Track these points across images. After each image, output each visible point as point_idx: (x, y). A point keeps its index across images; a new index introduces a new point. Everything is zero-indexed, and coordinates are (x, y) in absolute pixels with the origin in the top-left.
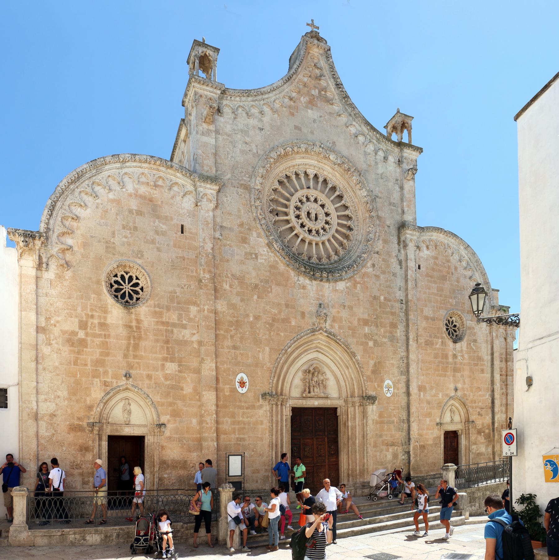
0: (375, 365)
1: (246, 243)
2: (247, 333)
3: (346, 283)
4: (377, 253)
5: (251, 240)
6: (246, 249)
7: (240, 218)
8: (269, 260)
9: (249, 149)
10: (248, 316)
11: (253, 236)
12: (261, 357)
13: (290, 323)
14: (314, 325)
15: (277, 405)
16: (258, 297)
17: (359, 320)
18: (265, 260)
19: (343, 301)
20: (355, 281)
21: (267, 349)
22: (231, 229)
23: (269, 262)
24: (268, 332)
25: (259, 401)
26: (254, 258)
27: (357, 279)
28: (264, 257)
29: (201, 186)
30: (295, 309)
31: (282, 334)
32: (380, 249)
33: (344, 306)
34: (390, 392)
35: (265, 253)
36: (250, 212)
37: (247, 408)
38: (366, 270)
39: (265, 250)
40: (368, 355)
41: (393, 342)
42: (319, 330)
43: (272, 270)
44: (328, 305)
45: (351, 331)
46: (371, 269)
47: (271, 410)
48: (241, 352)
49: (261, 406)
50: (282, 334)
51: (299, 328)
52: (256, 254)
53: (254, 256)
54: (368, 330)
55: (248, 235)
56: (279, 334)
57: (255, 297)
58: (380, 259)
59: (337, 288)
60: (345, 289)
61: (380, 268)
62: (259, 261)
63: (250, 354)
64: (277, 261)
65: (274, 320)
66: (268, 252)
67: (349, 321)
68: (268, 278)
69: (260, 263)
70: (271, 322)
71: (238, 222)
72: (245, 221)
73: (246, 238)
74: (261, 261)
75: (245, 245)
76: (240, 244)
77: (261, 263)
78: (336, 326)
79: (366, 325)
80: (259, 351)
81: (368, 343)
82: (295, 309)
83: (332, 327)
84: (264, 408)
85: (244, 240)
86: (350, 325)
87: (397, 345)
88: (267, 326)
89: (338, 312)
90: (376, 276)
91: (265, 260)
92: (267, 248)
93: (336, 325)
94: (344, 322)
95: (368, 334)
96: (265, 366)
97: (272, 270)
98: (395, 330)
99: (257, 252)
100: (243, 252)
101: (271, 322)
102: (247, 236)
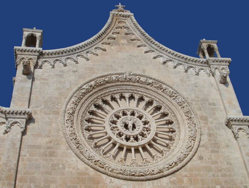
1: (54, 156)
3: (170, 178)
4: (203, 146)
6: (54, 161)
7: (49, 137)
22: (39, 147)
27: (182, 173)
29: (10, 118)
35: (73, 162)
36: (60, 131)
39: (74, 159)
46: (199, 162)
53: (61, 166)
59: (159, 185)
62: (67, 169)
64: (86, 168)
66: (77, 161)
68: (75, 184)
71: (47, 140)
72: (55, 138)
73: (54, 152)
75: (52, 158)
76: (48, 158)
85: (52, 154)
91: (74, 168)
92: (76, 157)
97: (80, 176)
100: (50, 165)
102: (56, 150)
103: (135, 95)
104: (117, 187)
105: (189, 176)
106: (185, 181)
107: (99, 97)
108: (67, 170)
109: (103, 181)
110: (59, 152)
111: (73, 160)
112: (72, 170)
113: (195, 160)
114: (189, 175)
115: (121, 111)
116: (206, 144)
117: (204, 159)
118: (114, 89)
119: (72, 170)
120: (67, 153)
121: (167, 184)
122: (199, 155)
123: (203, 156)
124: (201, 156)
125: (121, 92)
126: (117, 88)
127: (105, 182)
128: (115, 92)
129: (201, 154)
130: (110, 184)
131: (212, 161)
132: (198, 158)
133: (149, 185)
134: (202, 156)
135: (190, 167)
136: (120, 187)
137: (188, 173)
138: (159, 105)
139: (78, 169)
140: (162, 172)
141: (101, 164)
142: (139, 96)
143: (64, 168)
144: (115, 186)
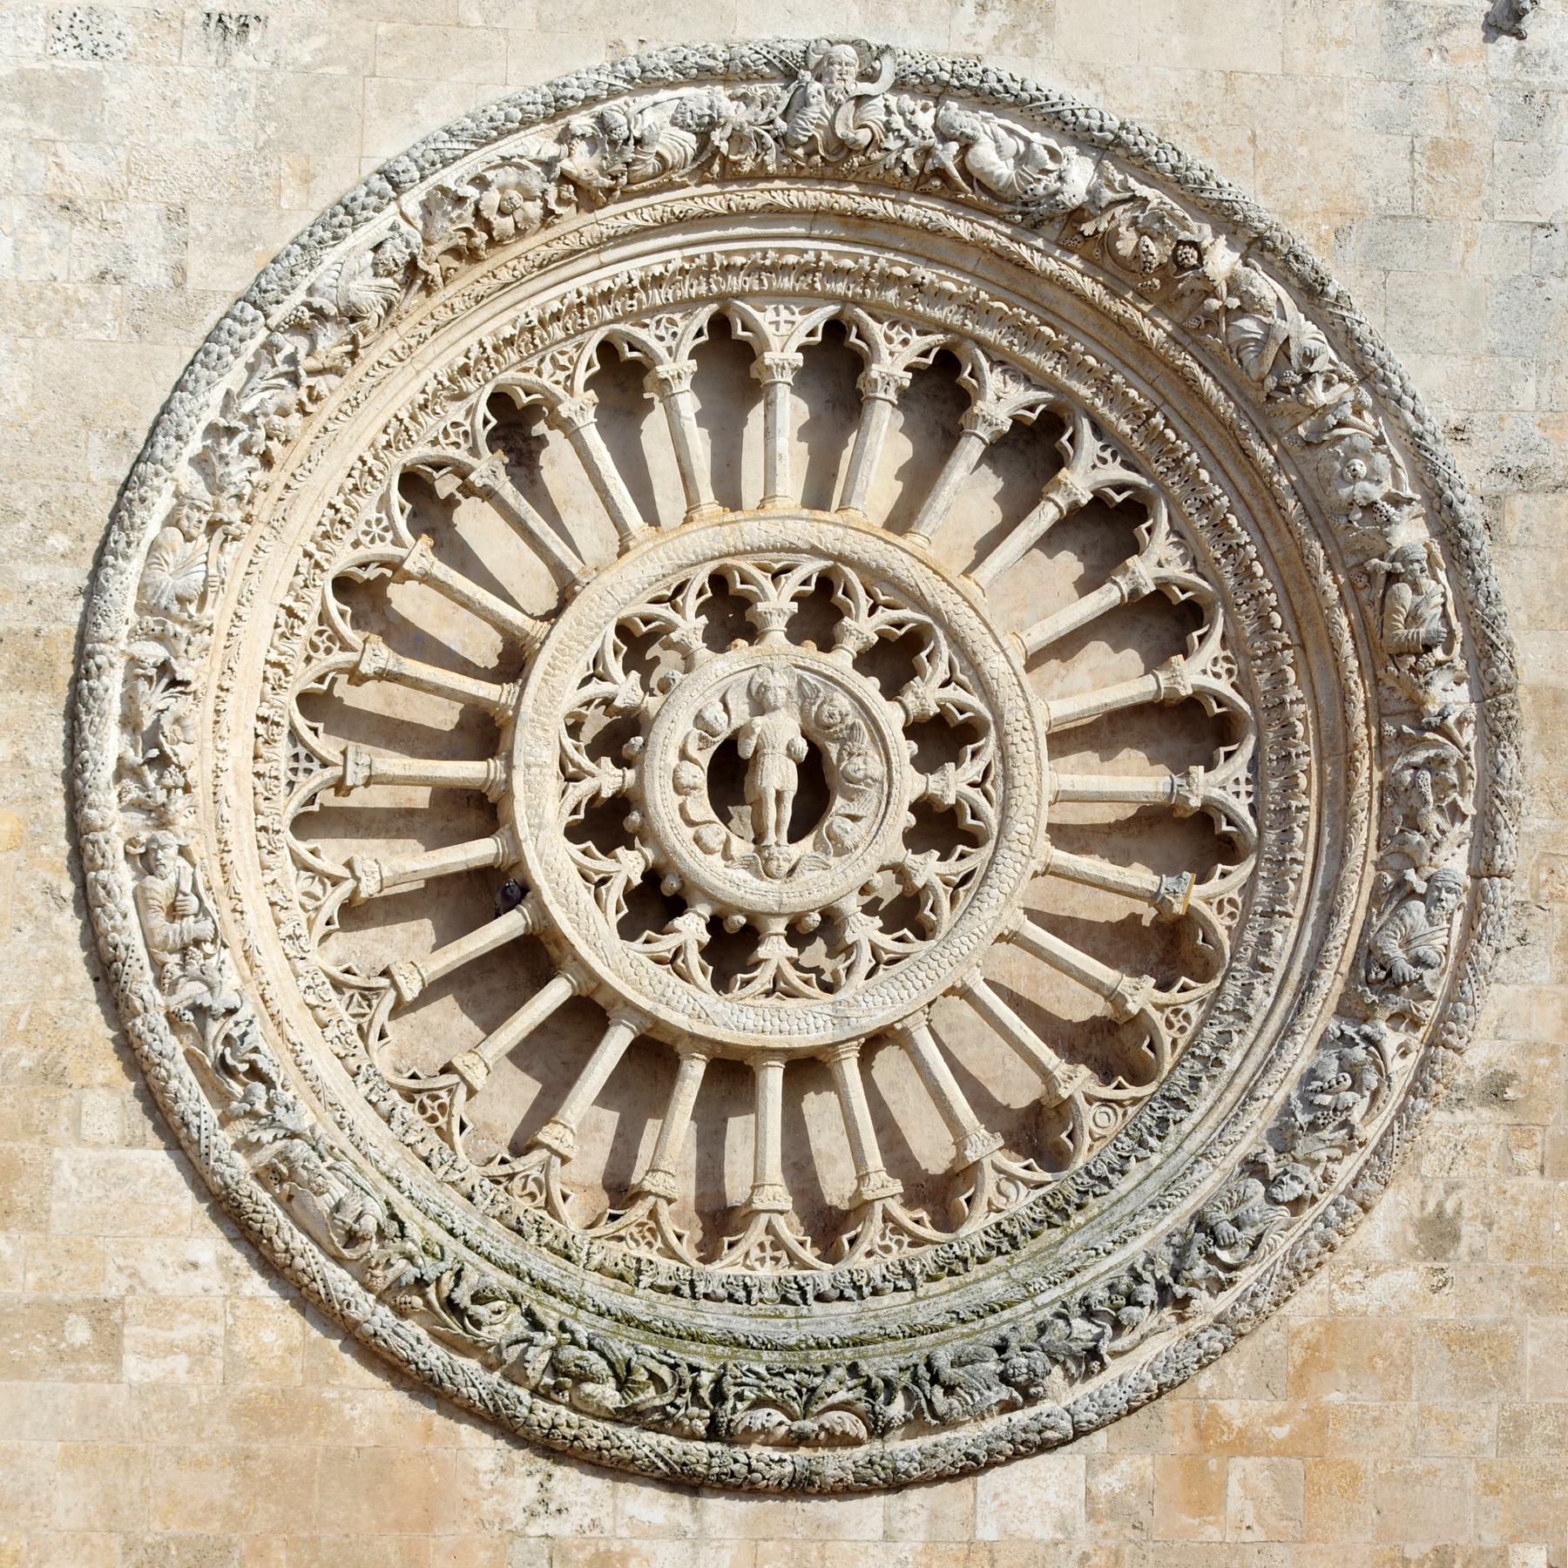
3: (1091, 1467)
5: (65, 1177)
8: (243, 1345)
9: (91, 265)
11: (88, 1132)
18: (200, 1354)
20: (1207, 1428)
23: (235, 1366)
26: (77, 1352)
27: (1231, 1409)
28: (187, 1330)
32: (1529, 1048)
35: (196, 1281)
38: (1343, 1300)
43: (262, 1447)
46: (1410, 1278)
52: (102, 1314)
55: (28, 1129)
58: (1525, 1157)
60: (1083, 1529)
61: (1512, 1250)
62: (134, 1368)
69: (141, 1393)
74: (157, 1370)
77: (155, 1388)
90: (1461, 1340)
91: (200, 1354)
97: (262, 1447)
99: (114, 1287)
102: (29, 1148)
103: (878, 330)
104: (597, 1554)
105: (1281, 1450)
106: (1234, 1488)
107: (467, 384)
108: (135, 1377)
109: (470, 1493)
110: (59, 1161)
111: (195, 1266)
112: (182, 1376)
113: (1384, 1254)
114: (1280, 1432)
115: (701, 577)
116: (1523, 1073)
117: (1463, 1249)
118: (634, 270)
119: (182, 1376)
120: (140, 1174)
121: (1062, 1526)
122: (1423, 1203)
123: (1466, 1213)
124: (1449, 1207)
125: (723, 298)
126: (680, 247)
127: (487, 1505)
128: (658, 296)
129: (1451, 1189)
130: (535, 1529)
131: (1533, 1272)
132: (1411, 1237)
133: (888, 1537)
134: (1458, 1212)
135: (1307, 1335)
136: (624, 1558)
137: (1279, 1407)
138: (1120, 488)
139: (235, 1366)
140: (1031, 1400)
141: (451, 1305)
142: (918, 342)
143: (109, 1346)
144: (581, 1548)
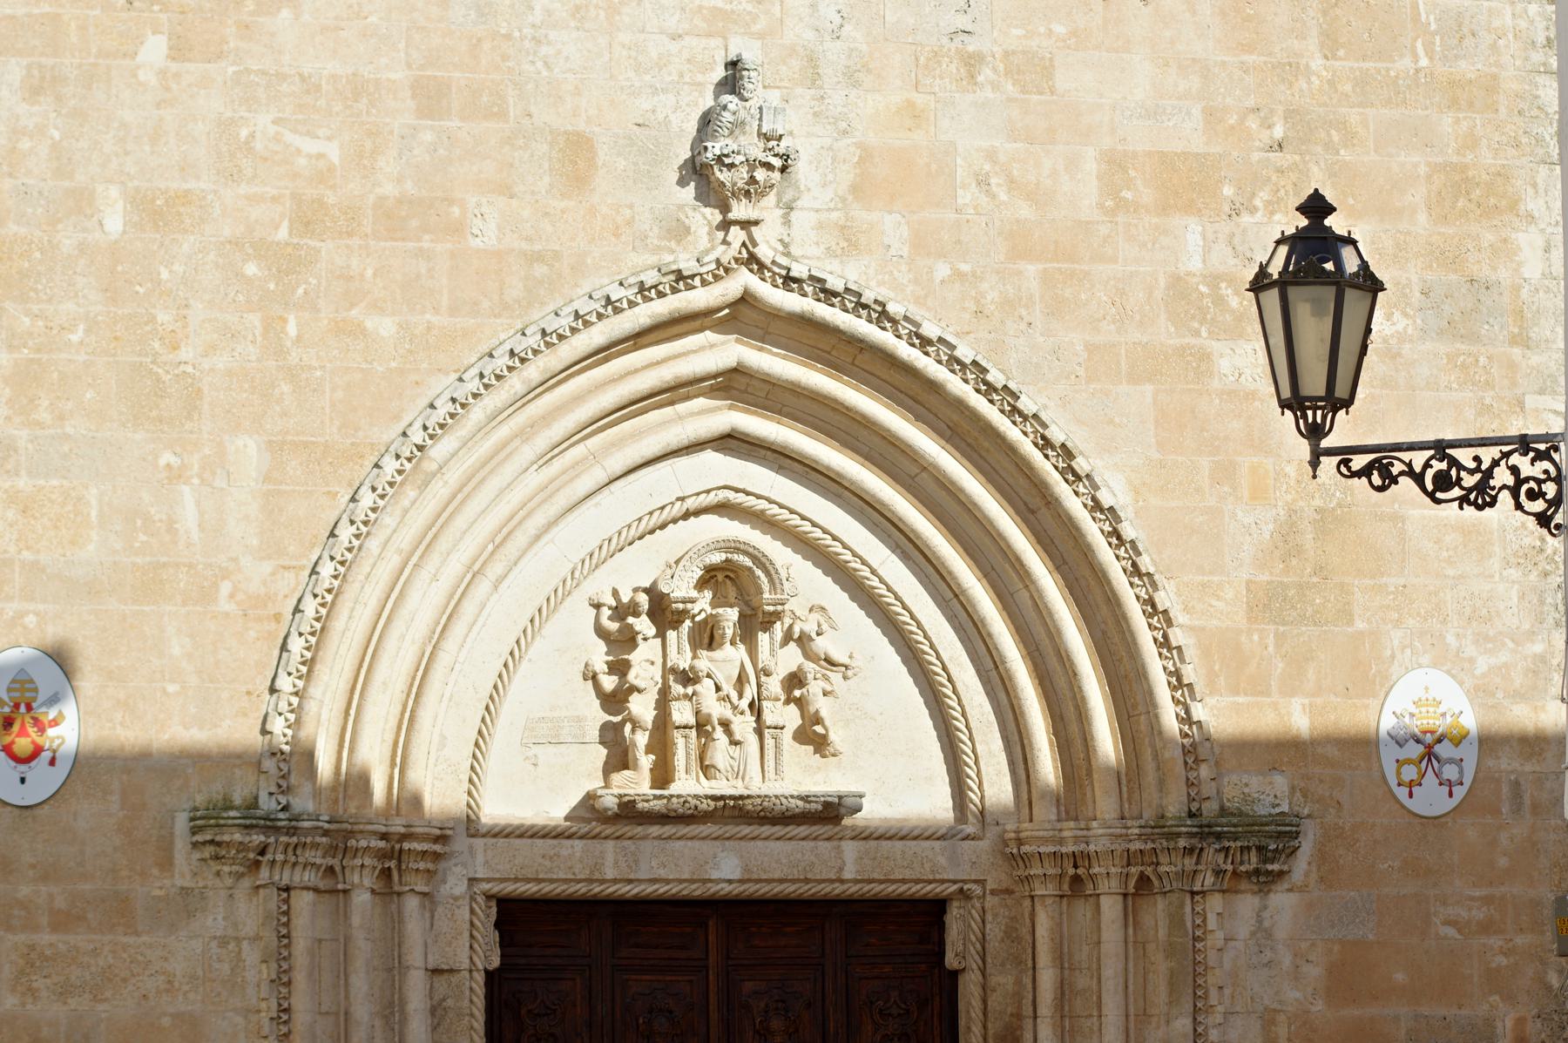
0: (1286, 542)
2: (75, 338)
10: (82, 203)
12: (188, 516)
13: (457, 229)
14: (680, 232)
15: (334, 891)
16: (179, 51)
17: (1116, 165)
19: (962, 22)
21: (248, 451)
24: (255, 319)
25: (167, 863)
30: (502, 115)
31: (384, 326)
33: (972, 63)
34: (1450, 772)
37: (63, 921)
40: (1205, 463)
41: (1473, 338)
42: (723, 270)
44: (812, 61)
45: (1031, 269)
47: (270, 937)
48: (23, 483)
49: (188, 903)
50: (384, 326)
51: (540, 270)
54: (1207, 250)
56: (359, 331)
57: (154, 49)
63: (92, 495)
65: (308, 219)
67: (1011, 182)
70: (283, 234)
78: (892, 228)
79: (1189, 208)
80: (176, 475)
81: (1205, 357)
82: (502, 115)
83: (849, 241)
84: (214, 921)
86: (1025, 212)
87: (1512, 366)
88: (251, 269)
89: (913, 115)
93: (889, 221)
94: (965, 197)
95: (1214, 280)
96: (225, 588)
98: (1489, 237)
101: (283, 234)
